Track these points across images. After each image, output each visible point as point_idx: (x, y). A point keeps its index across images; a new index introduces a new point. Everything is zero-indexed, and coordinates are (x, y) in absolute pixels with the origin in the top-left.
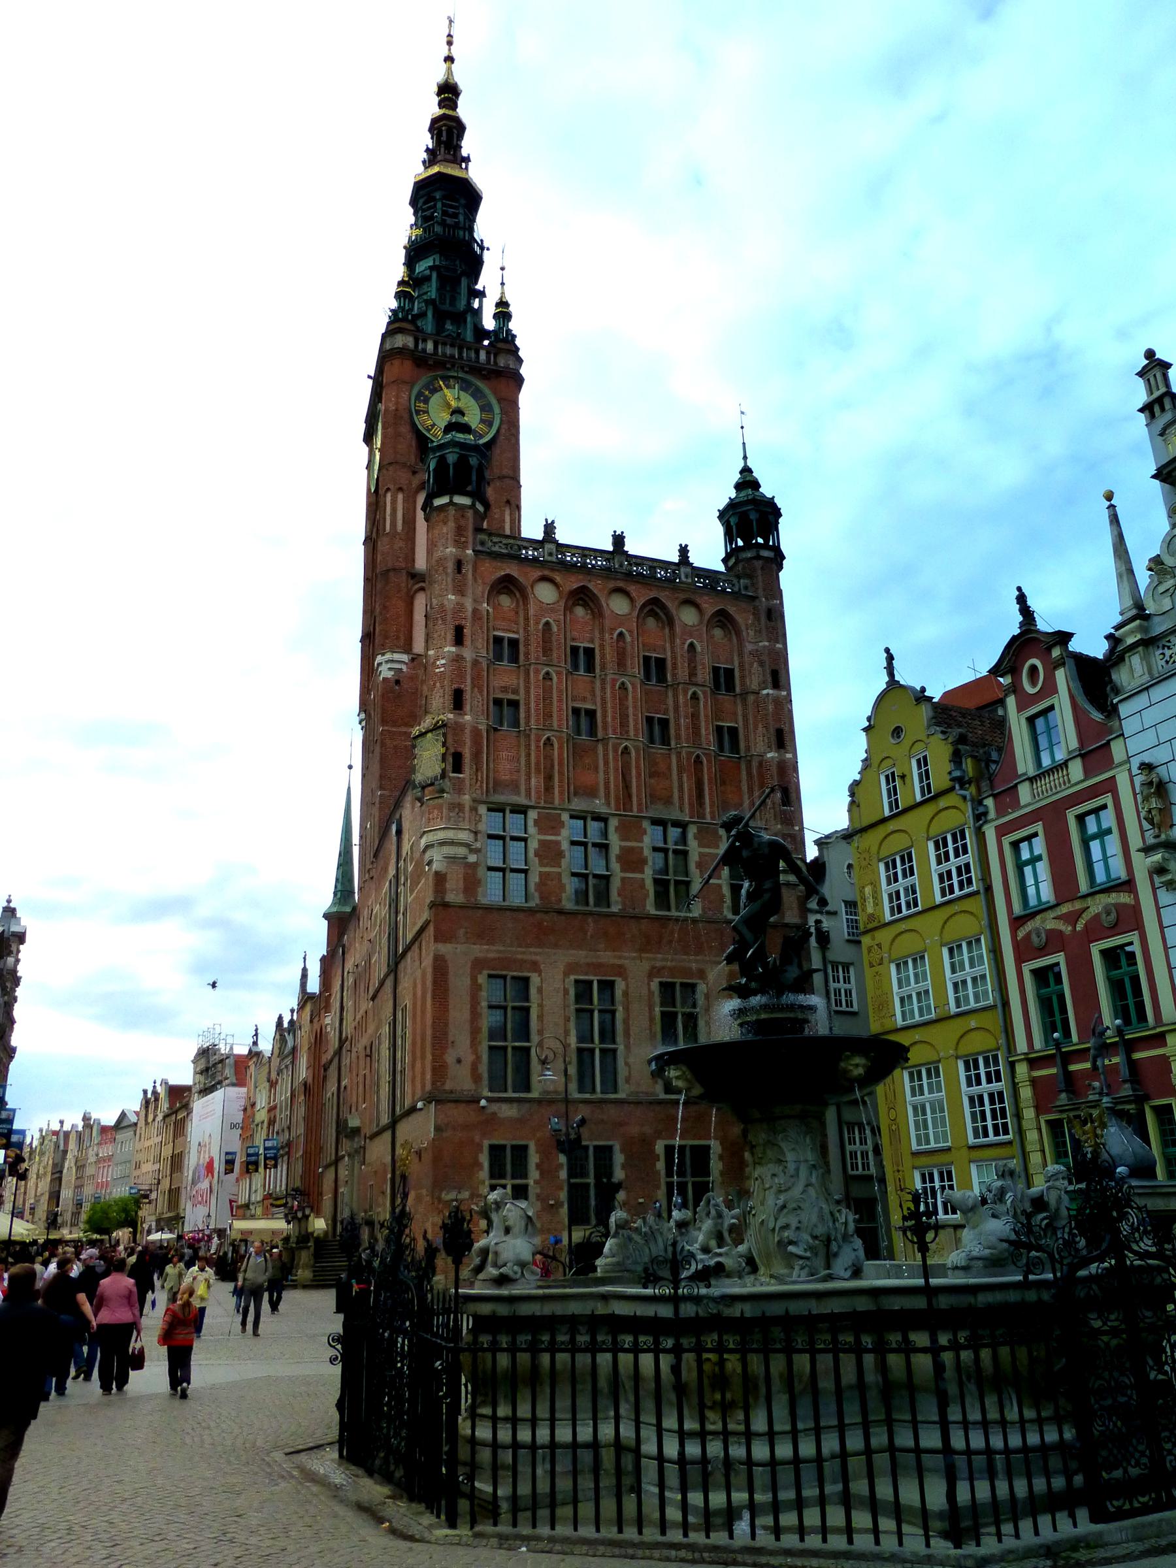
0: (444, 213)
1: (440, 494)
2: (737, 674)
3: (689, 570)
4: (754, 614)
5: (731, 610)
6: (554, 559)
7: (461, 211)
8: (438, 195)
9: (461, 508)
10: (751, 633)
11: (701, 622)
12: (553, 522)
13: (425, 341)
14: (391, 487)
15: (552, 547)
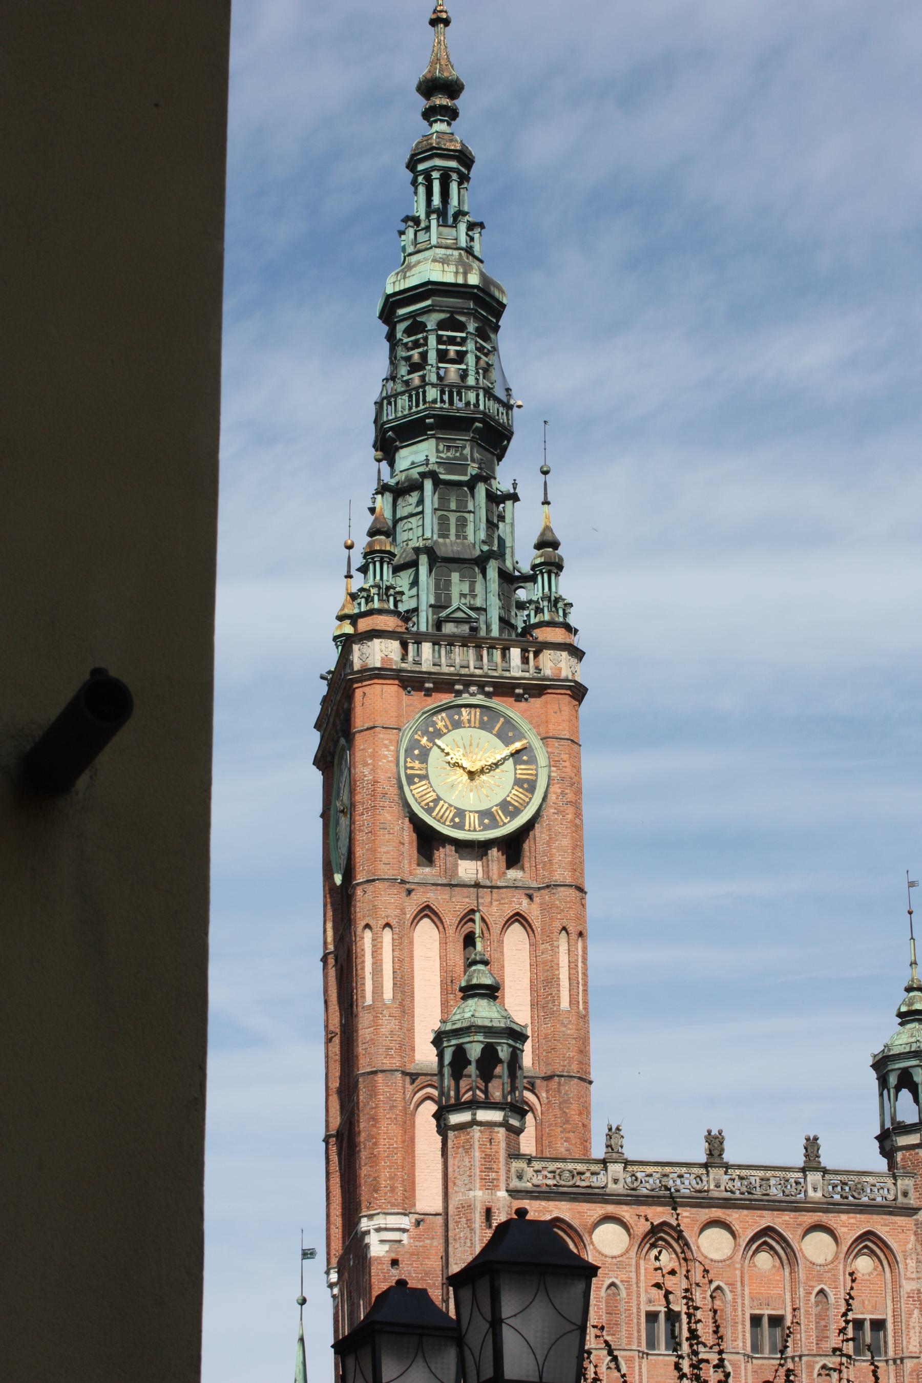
0: (442, 356)
1: (459, 1107)
2: (890, 1326)
3: (820, 1174)
4: (916, 1233)
5: (882, 1231)
6: (619, 1188)
7: (470, 346)
8: (431, 321)
9: (490, 1124)
10: (912, 1264)
11: (836, 1257)
12: (618, 1129)
13: (418, 643)
14: (372, 923)
15: (619, 1167)
